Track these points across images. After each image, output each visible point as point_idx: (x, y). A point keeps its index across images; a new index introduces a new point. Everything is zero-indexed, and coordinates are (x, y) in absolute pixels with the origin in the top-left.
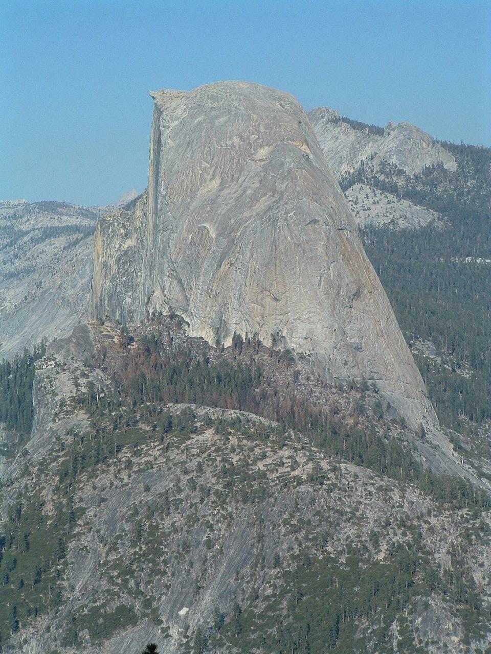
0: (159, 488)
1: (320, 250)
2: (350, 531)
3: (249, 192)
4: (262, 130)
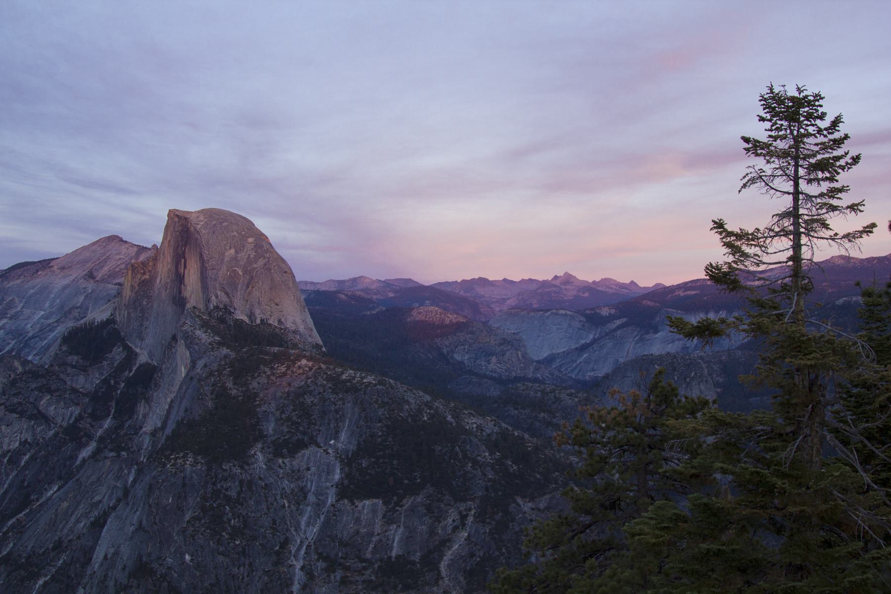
0: (296, 384)
1: (291, 285)
2: (407, 407)
3: (252, 256)
4: (246, 230)
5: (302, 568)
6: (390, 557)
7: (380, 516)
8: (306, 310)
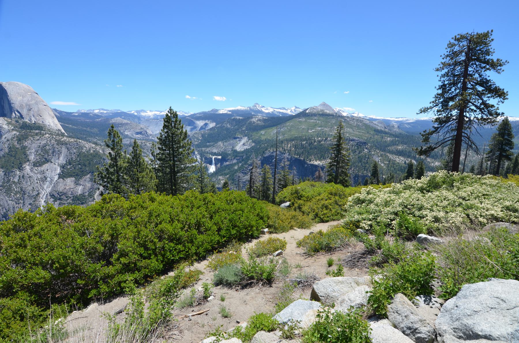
5: (44, 202)
6: (77, 195)
7: (73, 183)
8: (55, 118)
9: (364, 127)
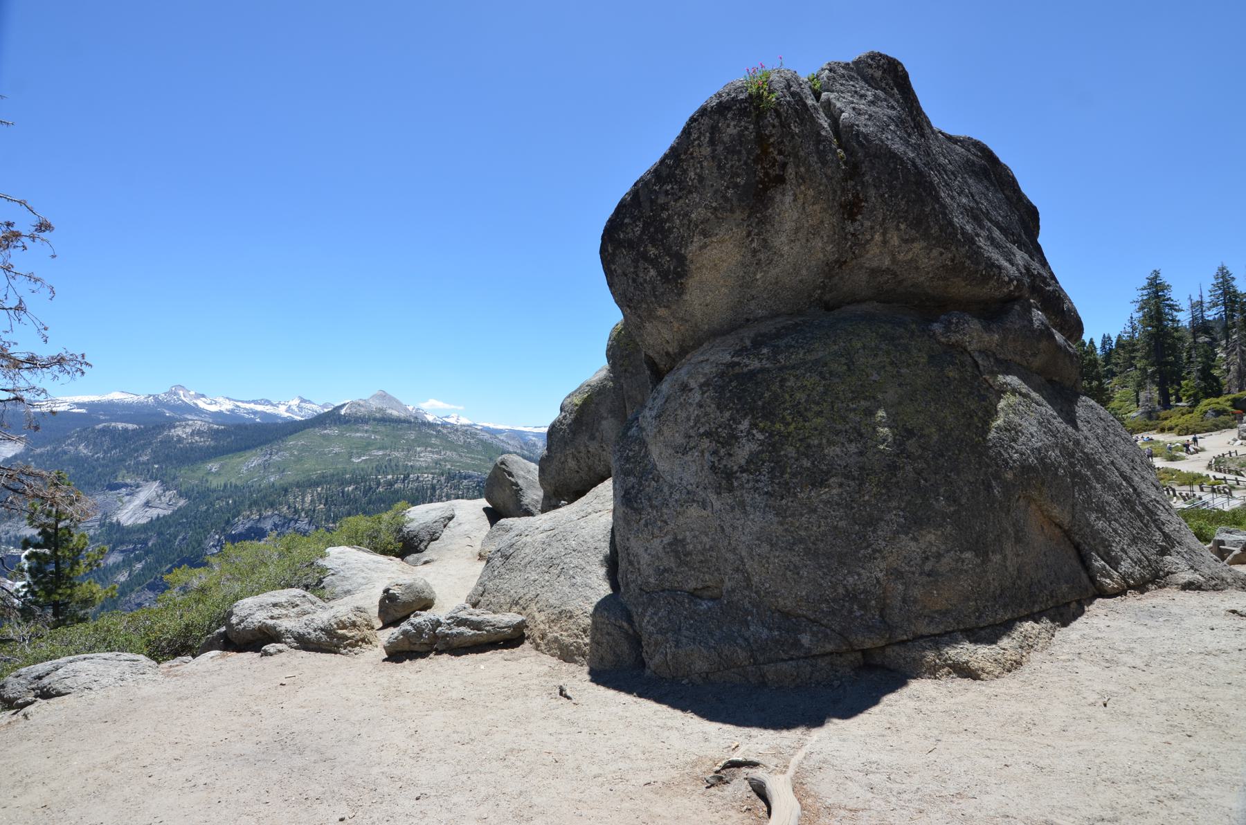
9: (480, 448)
